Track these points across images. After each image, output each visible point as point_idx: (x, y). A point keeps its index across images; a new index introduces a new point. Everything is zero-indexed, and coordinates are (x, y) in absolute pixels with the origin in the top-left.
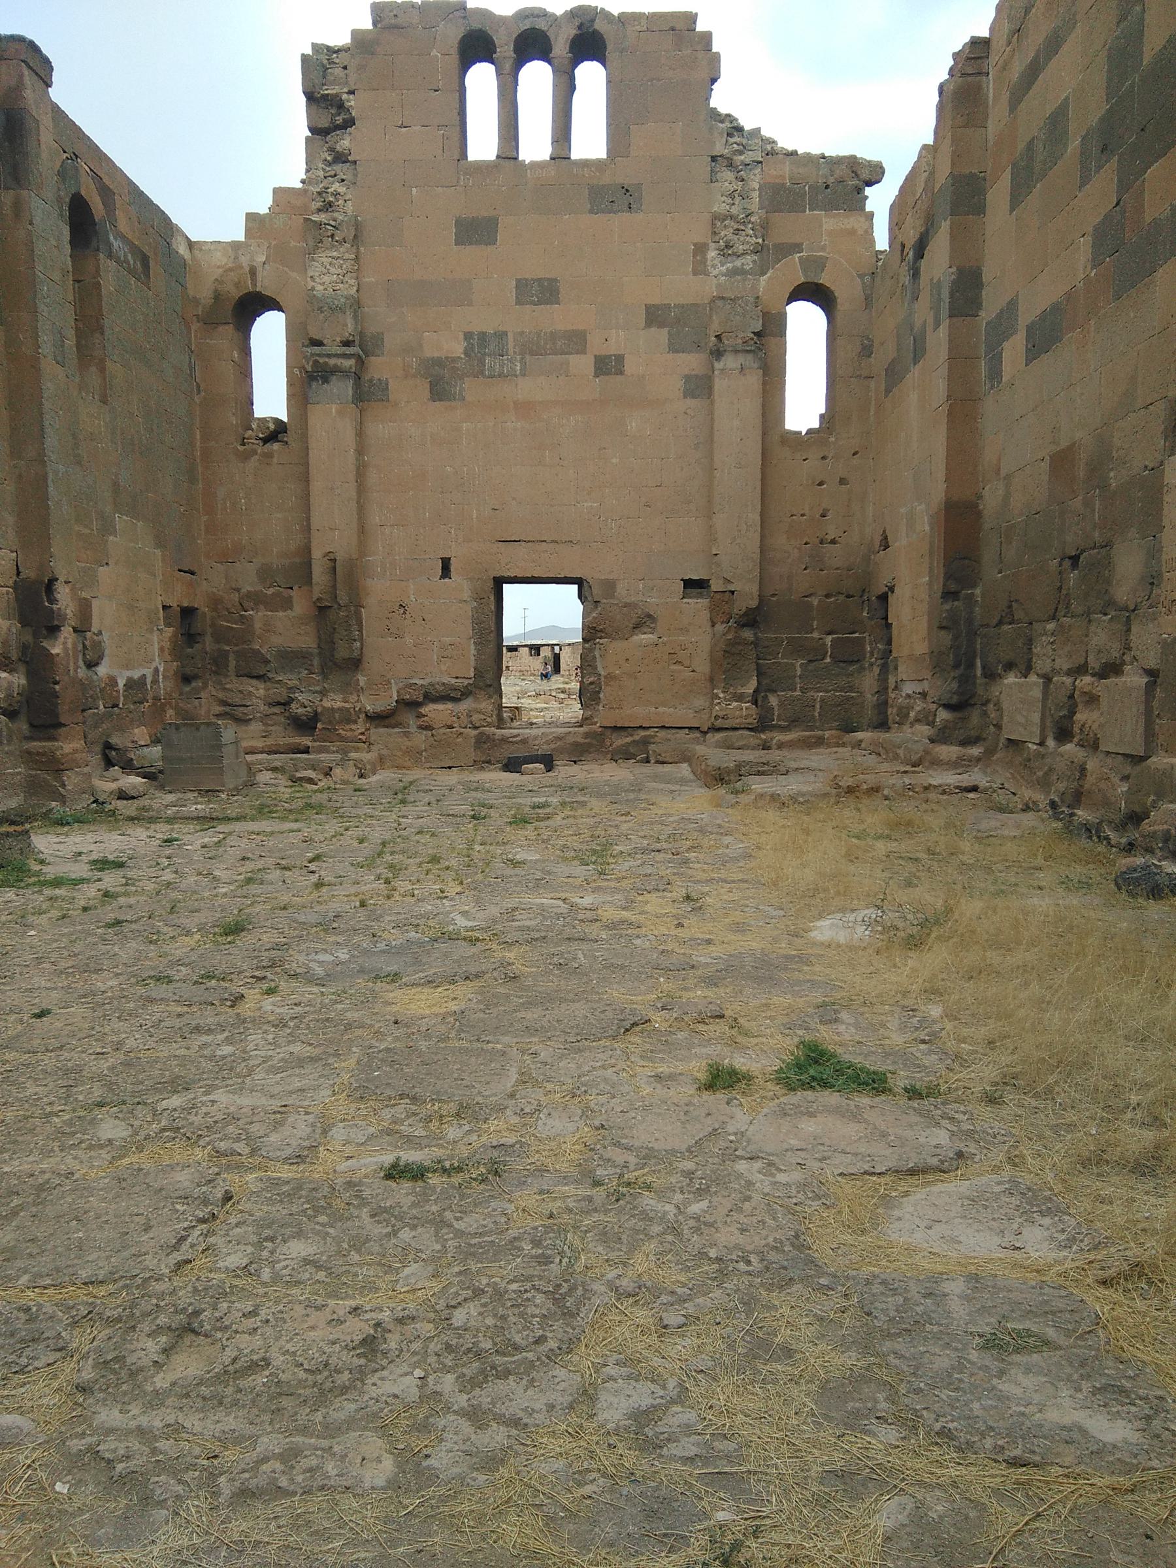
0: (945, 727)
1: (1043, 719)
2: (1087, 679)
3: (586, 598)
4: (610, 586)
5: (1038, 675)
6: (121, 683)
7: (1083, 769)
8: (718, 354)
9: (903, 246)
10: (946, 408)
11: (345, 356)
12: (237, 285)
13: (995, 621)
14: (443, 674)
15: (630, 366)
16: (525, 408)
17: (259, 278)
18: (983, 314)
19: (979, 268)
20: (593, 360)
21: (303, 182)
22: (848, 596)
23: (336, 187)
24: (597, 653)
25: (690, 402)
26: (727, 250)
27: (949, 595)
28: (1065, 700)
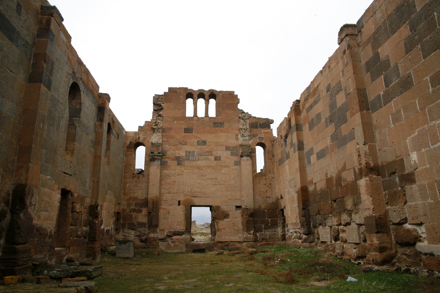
0: (305, 239)
1: (331, 236)
2: (341, 227)
3: (212, 210)
4: (218, 207)
5: (328, 226)
6: (105, 230)
7: (343, 247)
8: (242, 156)
9: (281, 136)
10: (299, 169)
12: (135, 140)
13: (315, 215)
16: (199, 168)
18: (305, 150)
19: (303, 141)
20: (214, 157)
21: (151, 120)
22: (273, 210)
23: (159, 121)
24: (215, 223)
25: (236, 167)
26: (243, 136)
27: (303, 209)
28: (337, 231)
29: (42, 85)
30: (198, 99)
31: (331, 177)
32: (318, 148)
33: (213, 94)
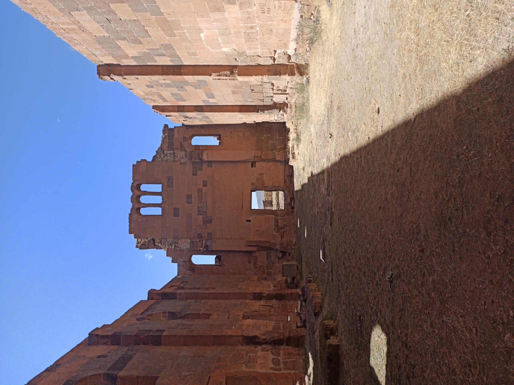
4: (253, 184)
6: (274, 288)
11: (202, 241)
14: (273, 223)
15: (205, 180)
17: (186, 260)
20: (204, 187)
21: (165, 250)
25: (213, 166)
29: (163, 334)
30: (141, 203)
31: (232, 91)
32: (204, 97)
33: (136, 187)
